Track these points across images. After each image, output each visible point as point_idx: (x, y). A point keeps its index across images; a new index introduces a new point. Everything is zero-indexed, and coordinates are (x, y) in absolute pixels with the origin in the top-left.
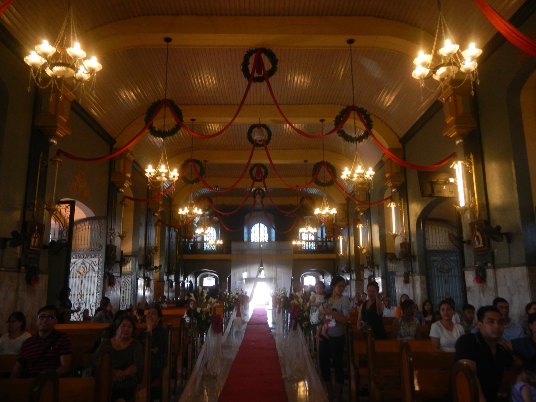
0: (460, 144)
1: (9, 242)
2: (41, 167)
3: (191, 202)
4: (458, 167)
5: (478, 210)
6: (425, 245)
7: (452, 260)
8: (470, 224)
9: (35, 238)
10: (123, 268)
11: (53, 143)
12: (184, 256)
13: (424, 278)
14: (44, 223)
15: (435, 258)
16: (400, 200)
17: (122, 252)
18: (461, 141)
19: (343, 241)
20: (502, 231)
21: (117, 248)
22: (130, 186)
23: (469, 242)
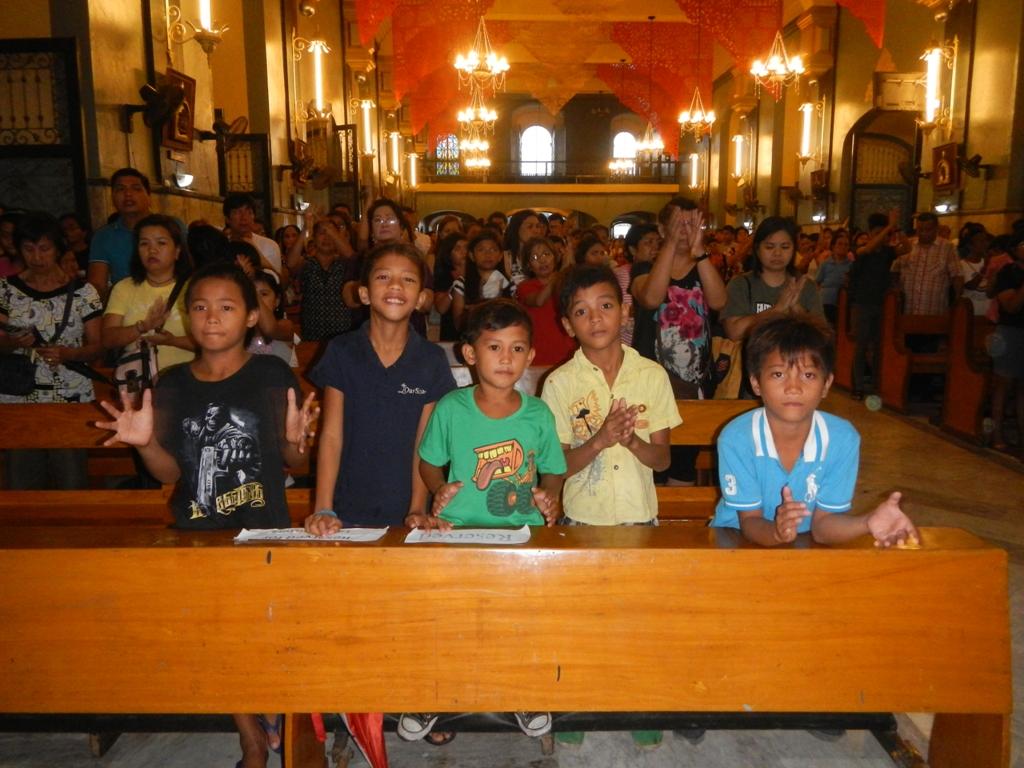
0: (942, 18)
3: (478, 99)
4: (933, 58)
5: (950, 127)
6: (854, 177)
7: (893, 201)
11: (309, 12)
15: (867, 197)
16: (821, 98)
18: (944, 14)
19: (699, 161)
20: (982, 163)
23: (928, 176)
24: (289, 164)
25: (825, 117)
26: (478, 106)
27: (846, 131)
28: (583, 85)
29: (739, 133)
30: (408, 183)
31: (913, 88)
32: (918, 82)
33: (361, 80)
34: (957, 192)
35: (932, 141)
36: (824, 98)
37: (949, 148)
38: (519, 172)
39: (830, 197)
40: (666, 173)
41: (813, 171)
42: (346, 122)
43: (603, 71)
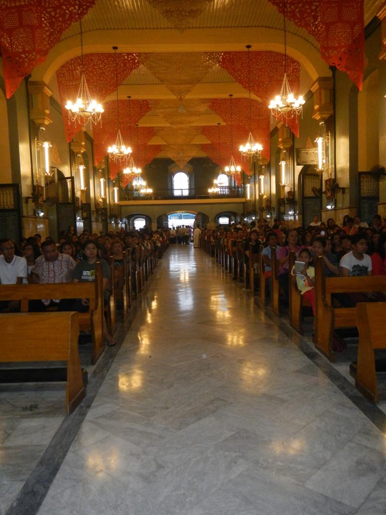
0: (323, 124)
1: (30, 200)
2: (37, 147)
4: (320, 141)
6: (303, 194)
11: (42, 130)
12: (120, 202)
13: (301, 216)
14: (43, 186)
18: (323, 123)
19: (251, 187)
24: (31, 196)
25: (291, 167)
29: (263, 175)
30: (114, 201)
32: (315, 152)
34: (334, 200)
35: (325, 177)
37: (329, 180)
38: (172, 194)
40: (240, 193)
42: (71, 175)
43: (204, 147)
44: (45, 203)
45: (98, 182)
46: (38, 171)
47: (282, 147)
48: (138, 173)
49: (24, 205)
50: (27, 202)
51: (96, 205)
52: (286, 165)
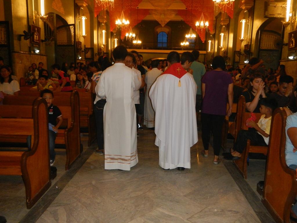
1: (23, 38)
8: (289, 33)
9: (36, 35)
10: (86, 55)
14: (40, 27)
16: (249, 18)
17: (85, 46)
19: (211, 43)
21: (82, 43)
22: (87, 6)
23: (286, 45)
24: (24, 34)
26: (122, 19)
27: (257, 29)
28: (173, 17)
29: (223, 32)
31: (281, 8)
32: (283, 6)
33: (82, 9)
35: (289, 29)
36: (250, 18)
39: (251, 54)
41: (245, 44)
43: (179, 12)
44: (44, 42)
45: (101, 33)
46: (35, 13)
47: (244, 8)
48: (127, 24)
49: (16, 42)
50: (19, 39)
51: (98, 50)
52: (246, 23)
